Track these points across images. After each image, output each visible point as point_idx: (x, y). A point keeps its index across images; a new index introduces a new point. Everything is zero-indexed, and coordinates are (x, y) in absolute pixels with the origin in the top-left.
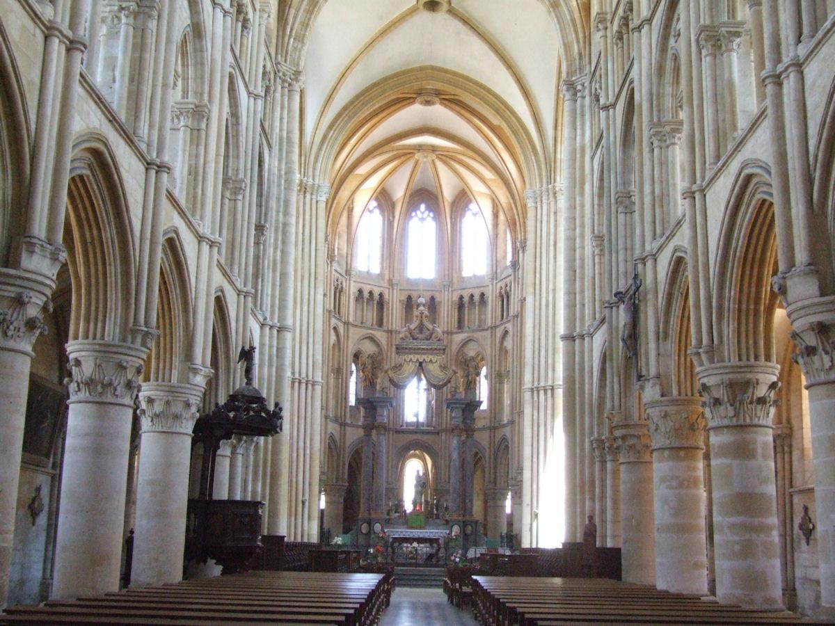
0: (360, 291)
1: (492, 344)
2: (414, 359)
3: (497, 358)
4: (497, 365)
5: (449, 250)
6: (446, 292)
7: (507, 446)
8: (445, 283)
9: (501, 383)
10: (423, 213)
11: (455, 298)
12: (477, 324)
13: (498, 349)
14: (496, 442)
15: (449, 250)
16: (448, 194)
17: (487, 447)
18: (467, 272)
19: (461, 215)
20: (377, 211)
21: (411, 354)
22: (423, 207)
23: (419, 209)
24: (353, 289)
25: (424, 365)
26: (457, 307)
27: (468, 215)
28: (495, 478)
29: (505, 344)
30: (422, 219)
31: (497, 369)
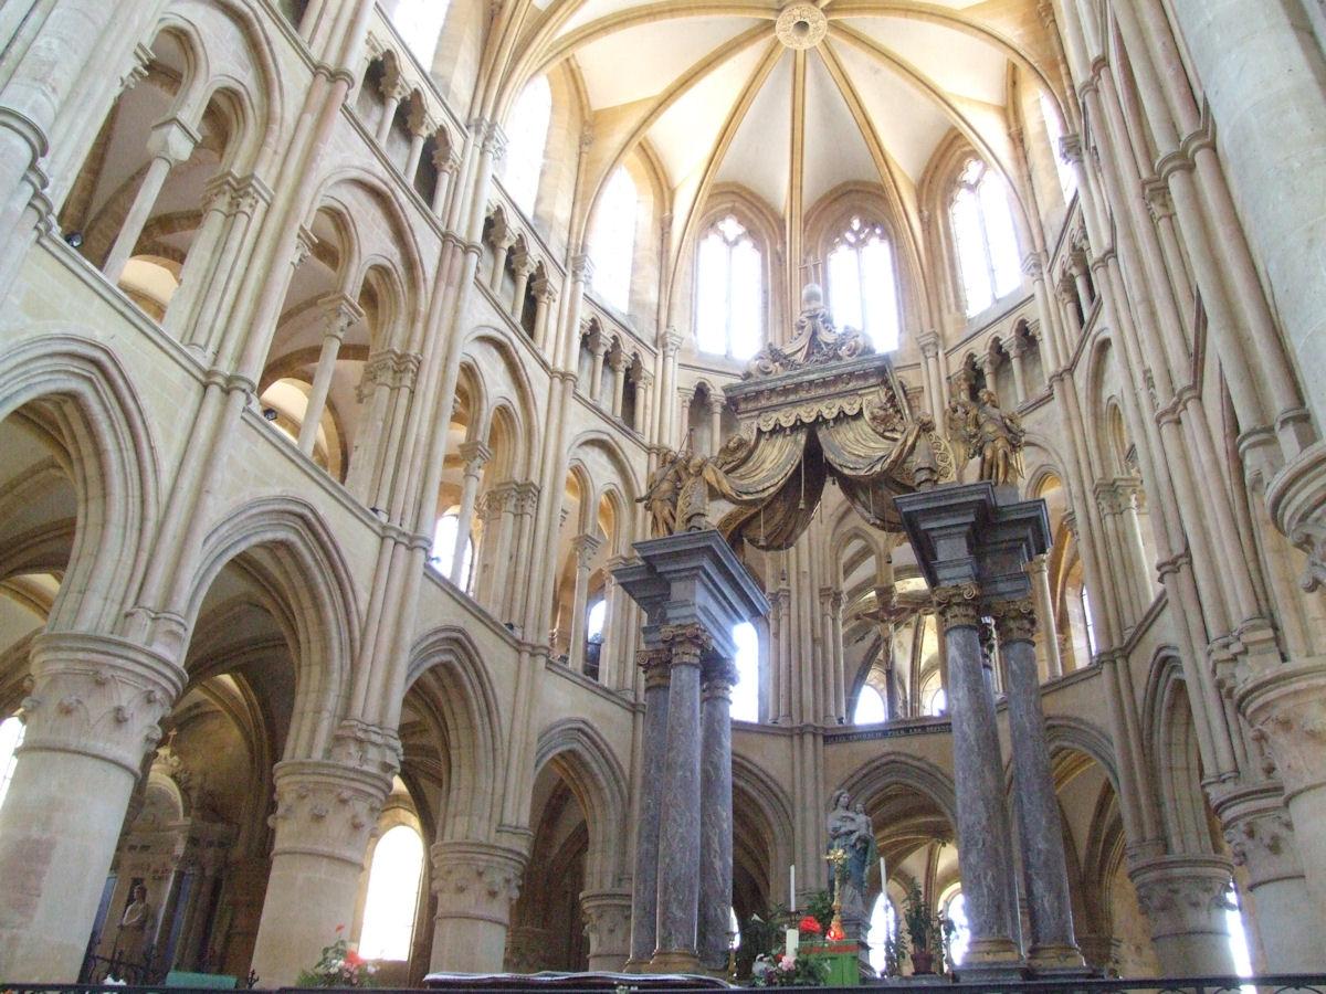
0: (701, 392)
1: (1069, 419)
2: (787, 422)
3: (1092, 444)
7: (1180, 686)
8: (924, 341)
9: (1119, 511)
10: (857, 234)
11: (957, 363)
13: (1088, 422)
14: (1140, 693)
16: (903, 160)
17: (1113, 731)
19: (944, 196)
20: (746, 245)
21: (775, 408)
22: (856, 224)
23: (848, 227)
25: (822, 434)
26: (964, 386)
27: (962, 195)
28: (1160, 823)
29: (1106, 394)
30: (860, 243)
31: (1098, 473)
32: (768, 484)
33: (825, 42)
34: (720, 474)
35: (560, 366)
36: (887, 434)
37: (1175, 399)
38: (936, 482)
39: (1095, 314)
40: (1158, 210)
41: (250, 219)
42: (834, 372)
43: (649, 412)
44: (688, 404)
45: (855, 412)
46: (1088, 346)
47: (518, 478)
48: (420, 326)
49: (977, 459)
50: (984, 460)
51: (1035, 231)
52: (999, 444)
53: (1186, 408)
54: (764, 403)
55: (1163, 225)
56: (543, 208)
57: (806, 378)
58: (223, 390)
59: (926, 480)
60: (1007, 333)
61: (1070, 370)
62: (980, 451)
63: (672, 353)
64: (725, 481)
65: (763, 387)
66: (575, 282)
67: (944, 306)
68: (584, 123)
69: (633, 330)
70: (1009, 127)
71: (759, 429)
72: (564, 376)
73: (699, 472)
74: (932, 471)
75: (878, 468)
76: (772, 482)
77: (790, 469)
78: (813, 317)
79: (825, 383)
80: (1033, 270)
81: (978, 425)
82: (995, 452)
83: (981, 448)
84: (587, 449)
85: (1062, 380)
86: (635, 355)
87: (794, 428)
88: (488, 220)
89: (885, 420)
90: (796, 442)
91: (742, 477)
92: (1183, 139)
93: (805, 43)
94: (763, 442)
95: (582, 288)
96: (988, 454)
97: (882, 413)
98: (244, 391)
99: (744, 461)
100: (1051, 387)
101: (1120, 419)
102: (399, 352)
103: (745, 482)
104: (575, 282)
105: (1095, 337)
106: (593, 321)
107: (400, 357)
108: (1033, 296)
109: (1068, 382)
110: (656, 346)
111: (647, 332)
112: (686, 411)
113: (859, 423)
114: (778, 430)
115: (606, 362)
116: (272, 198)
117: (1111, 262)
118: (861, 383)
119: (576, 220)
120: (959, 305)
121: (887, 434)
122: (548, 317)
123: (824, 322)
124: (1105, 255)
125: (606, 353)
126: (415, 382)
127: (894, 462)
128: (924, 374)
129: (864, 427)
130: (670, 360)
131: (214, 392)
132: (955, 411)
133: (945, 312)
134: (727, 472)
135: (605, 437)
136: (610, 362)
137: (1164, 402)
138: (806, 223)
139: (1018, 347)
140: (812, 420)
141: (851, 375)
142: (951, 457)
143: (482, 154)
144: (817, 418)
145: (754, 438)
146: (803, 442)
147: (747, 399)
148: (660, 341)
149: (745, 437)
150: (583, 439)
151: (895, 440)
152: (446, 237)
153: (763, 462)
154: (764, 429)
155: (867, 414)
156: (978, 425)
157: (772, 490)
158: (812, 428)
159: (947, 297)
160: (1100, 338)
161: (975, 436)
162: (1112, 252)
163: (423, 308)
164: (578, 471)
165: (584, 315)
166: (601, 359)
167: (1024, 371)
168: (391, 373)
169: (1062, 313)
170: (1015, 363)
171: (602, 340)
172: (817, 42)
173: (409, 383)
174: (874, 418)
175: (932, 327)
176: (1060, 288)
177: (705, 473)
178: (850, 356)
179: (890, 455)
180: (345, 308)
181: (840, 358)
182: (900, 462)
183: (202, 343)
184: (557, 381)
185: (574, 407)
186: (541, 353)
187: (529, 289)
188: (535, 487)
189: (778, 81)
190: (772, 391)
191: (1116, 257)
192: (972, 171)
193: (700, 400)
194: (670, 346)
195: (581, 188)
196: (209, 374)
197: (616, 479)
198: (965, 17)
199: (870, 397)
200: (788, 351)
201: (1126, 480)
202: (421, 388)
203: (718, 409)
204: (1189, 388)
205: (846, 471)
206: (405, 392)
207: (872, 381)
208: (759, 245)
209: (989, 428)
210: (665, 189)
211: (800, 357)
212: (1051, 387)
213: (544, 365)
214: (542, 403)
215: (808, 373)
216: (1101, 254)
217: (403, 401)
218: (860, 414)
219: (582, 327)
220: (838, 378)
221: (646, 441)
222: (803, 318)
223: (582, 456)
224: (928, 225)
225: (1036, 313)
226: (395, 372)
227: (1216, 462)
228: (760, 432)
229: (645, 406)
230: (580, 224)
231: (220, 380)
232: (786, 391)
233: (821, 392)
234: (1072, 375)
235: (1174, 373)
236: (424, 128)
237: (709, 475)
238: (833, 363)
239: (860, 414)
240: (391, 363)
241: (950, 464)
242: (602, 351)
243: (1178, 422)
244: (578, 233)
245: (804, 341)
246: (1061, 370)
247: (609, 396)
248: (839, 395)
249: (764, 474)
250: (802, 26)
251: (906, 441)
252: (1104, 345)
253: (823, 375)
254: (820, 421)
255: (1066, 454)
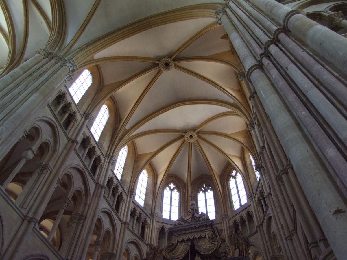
0: (163, 229)
1: (262, 238)
4: (271, 252)
5: (223, 199)
6: (225, 222)
11: (231, 222)
12: (249, 233)
15: (223, 199)
18: (236, 206)
20: (176, 190)
24: (156, 225)
25: (195, 242)
26: (233, 229)
29: (272, 231)
31: (271, 254)
32: (180, 256)
33: (197, 141)
34: (167, 253)
35: (124, 220)
36: (213, 243)
37: (290, 233)
38: (227, 256)
39: (267, 209)
40: (281, 184)
41: (45, 175)
42: (198, 225)
43: (148, 234)
44: (159, 232)
45: (204, 236)
46: (266, 218)
47: (110, 251)
48: (87, 207)
49: (238, 250)
50: (239, 251)
51: (250, 188)
52: (244, 245)
53: (293, 236)
54: (179, 233)
55: (282, 187)
56: (124, 178)
57: (191, 226)
58: (28, 221)
59: (224, 256)
60: (244, 214)
61: (262, 224)
62: (238, 247)
63: (155, 218)
64: (168, 255)
65: (179, 229)
66: (130, 198)
67: (228, 207)
68: (136, 157)
69: (145, 211)
70: (242, 162)
71: (178, 240)
72: (125, 223)
73: (161, 252)
74: (225, 253)
75: (210, 252)
76: (181, 256)
77: (186, 252)
78: (193, 210)
79: (196, 228)
80: (250, 198)
81: (238, 240)
82: (242, 248)
83: (239, 247)
84: (130, 244)
85: (260, 227)
86: (145, 218)
87: (188, 240)
88: (108, 180)
89: (212, 238)
90: (188, 244)
91: (173, 254)
92: (285, 166)
93: (192, 141)
94: (179, 244)
95: (132, 200)
96: (241, 248)
97: (211, 236)
98: (34, 222)
99: (174, 249)
100: (257, 229)
101: (276, 238)
102: (80, 214)
103: (173, 255)
104: (130, 198)
105: (267, 216)
106: (134, 208)
107: (80, 215)
108: (251, 205)
109: (261, 229)
110: (151, 216)
111: (149, 212)
112: (158, 234)
113: (205, 239)
114: (183, 241)
115: (137, 220)
116: (52, 170)
117: (270, 196)
118: (206, 228)
119: (132, 182)
120: (232, 206)
121: (213, 243)
122: (123, 207)
123: (196, 211)
124: (268, 194)
125: (137, 217)
126: (84, 222)
127: (215, 251)
128: (223, 225)
129: (207, 240)
130: (154, 220)
131: (26, 221)
132: (231, 236)
133: (228, 209)
134: (168, 253)
135: (135, 241)
136: (138, 220)
137: (287, 234)
138: (191, 185)
139: (247, 218)
140: (192, 238)
141: (203, 226)
142: (231, 249)
143: (109, 163)
144: (194, 237)
145: (176, 243)
146: (190, 244)
147: (175, 232)
148: (152, 215)
149: (174, 242)
150: (129, 241)
151: (215, 244)
152: (97, 184)
153: (179, 250)
154: (179, 240)
155: (207, 237)
156: (238, 240)
157: (181, 258)
158: (192, 240)
159: (228, 205)
160: (269, 216)
161: (237, 243)
162: (270, 194)
163: (89, 202)
164: (127, 250)
165: (132, 207)
166: (136, 219)
167: (249, 225)
168: (77, 220)
169: (258, 209)
170: (247, 223)
171: (136, 214)
172: (195, 140)
173: (82, 223)
174: (209, 238)
175: (225, 212)
176: (258, 203)
177: (162, 252)
178: (203, 220)
179: (214, 248)
180: (67, 201)
181: (200, 221)
182: (216, 250)
183: (25, 207)
184: (123, 224)
185: (127, 232)
186: (119, 216)
187: (118, 199)
188: (114, 255)
189: (185, 150)
190: (181, 230)
191: (271, 195)
192: (234, 173)
193: (162, 231)
194: (155, 216)
195: (134, 173)
196: (25, 216)
197: (137, 253)
198: (231, 136)
199: (208, 232)
200: (186, 219)
201: (279, 256)
202: (85, 224)
203: (167, 234)
204: (294, 230)
205: (202, 253)
206: (81, 225)
207: (209, 228)
208: (178, 191)
209: (241, 241)
210: (156, 175)
211: (189, 220)
212: (257, 229)
213: (120, 220)
214: (118, 230)
215: (191, 225)
216: (267, 194)
217: (80, 228)
218: (205, 237)
219: (131, 210)
220: (199, 227)
221: (147, 242)
222: (190, 210)
223: (128, 246)
224: (223, 186)
225: (252, 209)
226: (79, 219)
227: (303, 250)
228: (178, 241)
229: (147, 232)
230: (133, 183)
231: (28, 218)
232: (185, 230)
233: (195, 230)
234: (262, 226)
235: (289, 226)
236: (94, 156)
237: (163, 253)
238: (198, 222)
239: (205, 237)
240: (78, 217)
241: (230, 251)
242: (136, 217)
243: (292, 240)
244: (132, 185)
245: (190, 216)
246: (259, 225)
247: (137, 230)
248: (200, 231)
249: (179, 253)
250: (191, 137)
251: (218, 245)
252: (270, 218)
253: (195, 226)
254: (195, 238)
255: (262, 248)
